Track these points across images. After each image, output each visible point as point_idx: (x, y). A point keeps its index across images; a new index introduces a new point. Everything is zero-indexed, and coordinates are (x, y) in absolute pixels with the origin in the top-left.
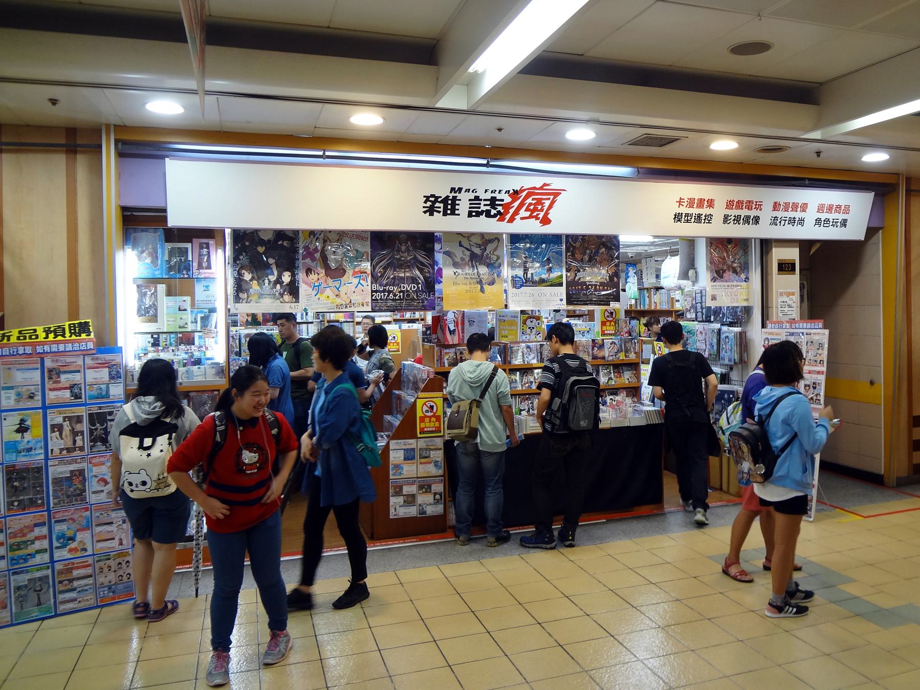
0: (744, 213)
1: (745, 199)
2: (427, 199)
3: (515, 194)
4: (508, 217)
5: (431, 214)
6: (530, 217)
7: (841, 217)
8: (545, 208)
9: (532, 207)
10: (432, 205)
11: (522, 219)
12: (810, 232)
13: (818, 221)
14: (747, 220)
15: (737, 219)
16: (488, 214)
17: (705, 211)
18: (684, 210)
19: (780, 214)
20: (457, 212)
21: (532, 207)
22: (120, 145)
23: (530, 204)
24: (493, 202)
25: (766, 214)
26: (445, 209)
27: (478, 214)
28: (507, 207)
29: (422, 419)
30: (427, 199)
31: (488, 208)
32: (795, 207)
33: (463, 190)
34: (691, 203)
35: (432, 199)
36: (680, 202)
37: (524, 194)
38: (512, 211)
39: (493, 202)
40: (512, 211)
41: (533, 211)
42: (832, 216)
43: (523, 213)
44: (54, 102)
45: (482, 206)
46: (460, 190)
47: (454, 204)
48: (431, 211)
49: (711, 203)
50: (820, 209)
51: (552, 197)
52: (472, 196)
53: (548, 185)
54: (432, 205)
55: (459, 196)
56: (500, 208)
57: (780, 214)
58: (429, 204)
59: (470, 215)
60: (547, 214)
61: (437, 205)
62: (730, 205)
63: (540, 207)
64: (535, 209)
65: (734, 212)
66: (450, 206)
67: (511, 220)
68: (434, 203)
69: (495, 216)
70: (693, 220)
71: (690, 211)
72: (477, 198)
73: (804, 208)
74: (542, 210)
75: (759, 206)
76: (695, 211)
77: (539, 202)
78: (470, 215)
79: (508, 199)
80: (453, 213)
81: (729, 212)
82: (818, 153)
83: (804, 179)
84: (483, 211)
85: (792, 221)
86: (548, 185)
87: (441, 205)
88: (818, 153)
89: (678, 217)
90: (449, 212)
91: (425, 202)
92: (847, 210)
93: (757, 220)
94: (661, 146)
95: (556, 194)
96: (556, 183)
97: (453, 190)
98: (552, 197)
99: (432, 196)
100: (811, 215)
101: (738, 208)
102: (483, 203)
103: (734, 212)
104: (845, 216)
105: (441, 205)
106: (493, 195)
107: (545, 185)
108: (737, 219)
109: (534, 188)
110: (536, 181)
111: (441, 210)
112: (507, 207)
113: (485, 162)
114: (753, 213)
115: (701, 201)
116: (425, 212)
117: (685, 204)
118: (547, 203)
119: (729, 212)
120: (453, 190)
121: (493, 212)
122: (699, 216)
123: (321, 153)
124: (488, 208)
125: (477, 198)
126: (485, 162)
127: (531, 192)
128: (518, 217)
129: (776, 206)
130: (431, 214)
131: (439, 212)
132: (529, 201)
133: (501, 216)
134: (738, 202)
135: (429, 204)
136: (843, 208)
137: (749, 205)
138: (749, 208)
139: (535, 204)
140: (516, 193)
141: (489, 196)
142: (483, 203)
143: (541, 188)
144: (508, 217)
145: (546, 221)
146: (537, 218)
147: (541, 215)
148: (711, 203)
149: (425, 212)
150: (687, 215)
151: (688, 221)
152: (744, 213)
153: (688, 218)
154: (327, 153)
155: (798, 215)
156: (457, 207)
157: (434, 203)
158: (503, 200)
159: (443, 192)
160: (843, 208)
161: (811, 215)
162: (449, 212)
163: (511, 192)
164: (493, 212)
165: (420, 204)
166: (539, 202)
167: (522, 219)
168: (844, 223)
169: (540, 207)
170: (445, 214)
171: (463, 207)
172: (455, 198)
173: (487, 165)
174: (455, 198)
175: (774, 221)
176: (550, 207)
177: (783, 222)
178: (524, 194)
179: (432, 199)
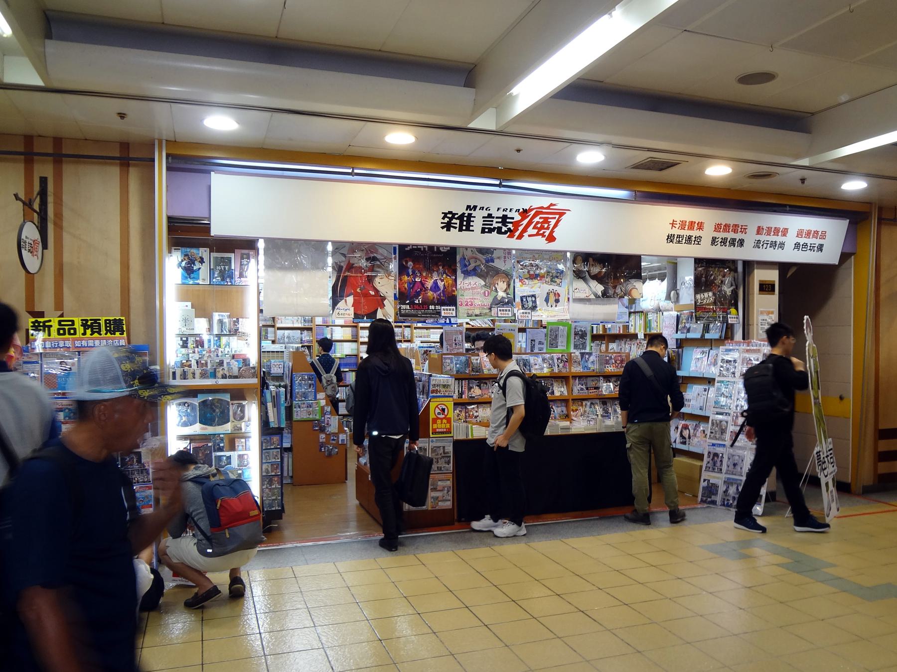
1: (732, 222)
2: (445, 215)
3: (525, 213)
4: (517, 234)
5: (448, 230)
6: (537, 234)
7: (818, 242)
8: (551, 227)
9: (539, 225)
10: (450, 221)
11: (530, 236)
12: (789, 255)
13: (797, 246)
14: (733, 242)
15: (724, 241)
16: (499, 231)
17: (695, 233)
18: (676, 231)
19: (763, 238)
20: (471, 228)
21: (539, 225)
22: (170, 158)
23: (538, 223)
24: (504, 218)
25: (750, 238)
26: (461, 225)
27: (491, 231)
28: (517, 224)
29: (435, 421)
30: (445, 215)
31: (500, 225)
32: (777, 231)
33: (478, 208)
34: (683, 225)
35: (450, 216)
36: (673, 224)
37: (532, 213)
38: (521, 228)
39: (504, 218)
40: (521, 228)
41: (540, 229)
42: (809, 241)
43: (531, 231)
44: (122, 116)
45: (494, 223)
46: (475, 207)
47: (469, 221)
48: (448, 226)
49: (701, 226)
50: (800, 234)
51: (557, 216)
52: (485, 213)
54: (450, 221)
55: (474, 213)
56: (510, 226)
57: (763, 238)
58: (446, 220)
59: (483, 231)
60: (552, 232)
61: (454, 221)
62: (718, 228)
63: (546, 225)
64: (542, 228)
65: (721, 235)
66: (465, 222)
67: (520, 237)
68: (451, 219)
69: (505, 233)
71: (682, 232)
72: (490, 216)
73: (785, 232)
74: (548, 228)
75: (744, 230)
76: (686, 233)
77: (546, 221)
78: (483, 231)
79: (517, 217)
80: (468, 229)
81: (716, 235)
82: (803, 180)
84: (495, 228)
85: (773, 245)
87: (458, 221)
88: (803, 180)
89: (670, 238)
90: (464, 228)
91: (443, 218)
92: (823, 235)
93: (741, 243)
94: (661, 170)
95: (561, 214)
96: (561, 203)
97: (468, 207)
98: (557, 216)
99: (450, 213)
100: (791, 239)
101: (725, 231)
102: (495, 220)
103: (721, 235)
105: (458, 221)
106: (505, 213)
107: (552, 205)
108: (724, 241)
109: (542, 208)
111: (458, 226)
112: (517, 224)
113: (497, 182)
114: (738, 236)
115: (692, 223)
116: (443, 228)
117: (677, 226)
118: (553, 222)
119: (716, 235)
120: (468, 207)
121: (504, 229)
122: (690, 237)
123: (350, 171)
124: (500, 225)
125: (490, 216)
126: (497, 182)
128: (526, 235)
129: (759, 230)
130: (448, 230)
131: (455, 228)
132: (537, 219)
133: (511, 233)
134: (725, 225)
135: (446, 220)
137: (735, 229)
138: (735, 231)
139: (542, 223)
140: (525, 212)
142: (495, 220)
143: (548, 208)
144: (517, 234)
145: (551, 239)
147: (547, 234)
148: (701, 226)
149: (443, 228)
150: (679, 236)
152: (730, 235)
153: (679, 239)
154: (356, 171)
155: (779, 239)
156: (472, 224)
157: (451, 219)
158: (513, 218)
159: (460, 210)
161: (791, 239)
162: (464, 228)
163: (521, 210)
164: (504, 229)
165: (439, 220)
166: (545, 221)
167: (530, 236)
168: (820, 248)
169: (546, 225)
170: (461, 230)
171: (477, 223)
172: (470, 215)
173: (500, 185)
174: (470, 215)
175: (758, 244)
176: (556, 225)
178: (532, 213)
179: (450, 216)
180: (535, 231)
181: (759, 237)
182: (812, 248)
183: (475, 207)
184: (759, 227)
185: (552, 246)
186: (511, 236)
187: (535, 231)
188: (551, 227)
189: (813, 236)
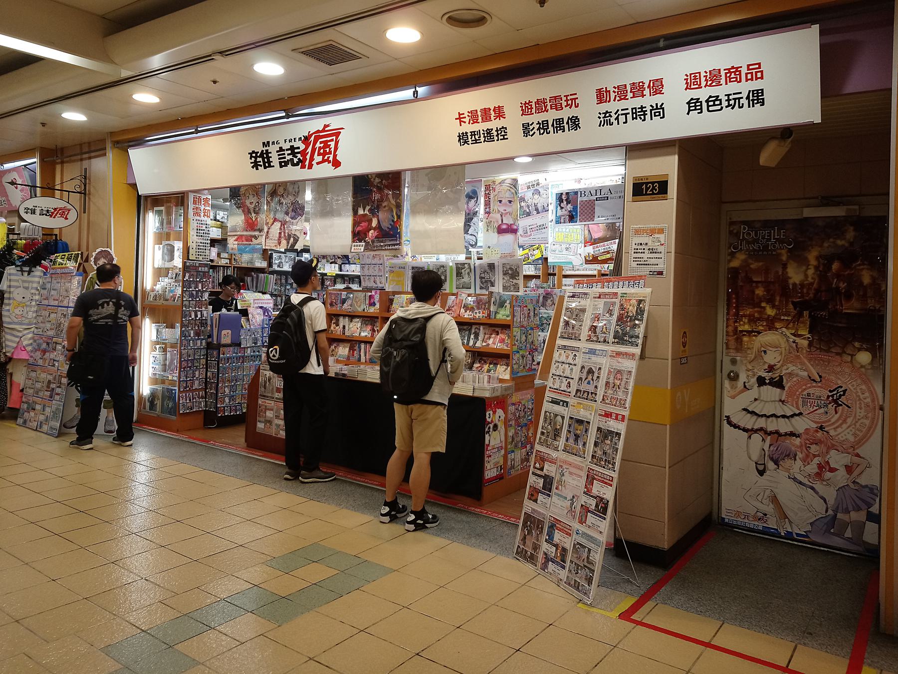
0: (551, 115)
3: (306, 140)
4: (307, 163)
5: (257, 169)
6: (323, 161)
7: (745, 87)
8: (332, 150)
9: (322, 151)
11: (318, 163)
13: (694, 105)
14: (559, 125)
16: (294, 165)
17: (494, 124)
18: (468, 128)
19: (613, 106)
21: (322, 151)
23: (320, 148)
24: (292, 148)
26: (264, 163)
28: (304, 153)
31: (291, 157)
32: (638, 89)
34: (474, 117)
36: (460, 118)
38: (308, 157)
39: (292, 148)
40: (308, 157)
42: (722, 91)
43: (318, 158)
46: (268, 142)
47: (268, 158)
49: (499, 112)
52: (277, 147)
53: (328, 126)
57: (613, 106)
59: (281, 166)
60: (335, 156)
62: (526, 109)
64: (325, 153)
65: (535, 118)
67: (310, 166)
69: (297, 164)
70: (482, 139)
72: (281, 149)
73: (657, 87)
74: (330, 153)
75: (572, 101)
76: (482, 126)
78: (281, 166)
79: (303, 147)
80: (270, 166)
81: (528, 119)
83: (656, 40)
85: (639, 113)
86: (328, 126)
87: (260, 159)
89: (463, 139)
92: (755, 71)
93: (575, 123)
96: (334, 122)
97: (264, 143)
99: (253, 152)
100: (675, 97)
101: (539, 110)
103: (535, 118)
104: (755, 85)
105: (260, 159)
106: (291, 144)
107: (326, 126)
108: (543, 127)
109: (318, 131)
110: (316, 125)
112: (304, 153)
114: (565, 114)
115: (486, 111)
117: (467, 120)
118: (332, 144)
119: (528, 119)
121: (296, 160)
122: (489, 131)
125: (281, 149)
127: (318, 135)
129: (602, 96)
130: (257, 169)
132: (318, 145)
133: (301, 162)
134: (538, 102)
136: (744, 70)
137: (556, 103)
138: (558, 107)
139: (324, 148)
141: (287, 146)
142: (287, 153)
143: (323, 131)
144: (307, 163)
145: (337, 164)
146: (329, 162)
147: (331, 159)
148: (499, 112)
150: (473, 134)
151: (476, 142)
152: (551, 115)
155: (648, 101)
157: (256, 157)
158: (298, 148)
159: (259, 149)
160: (744, 70)
161: (675, 97)
164: (296, 160)
165: (248, 162)
166: (324, 145)
167: (318, 163)
168: (757, 97)
170: (265, 167)
171: (275, 159)
172: (267, 151)
173: (287, 117)
174: (267, 151)
176: (336, 148)
177: (622, 119)
180: (320, 158)
181: (604, 107)
182: (734, 102)
183: (268, 142)
184: (599, 91)
185: (339, 172)
186: (303, 167)
187: (320, 158)
188: (332, 150)
189: (728, 80)
